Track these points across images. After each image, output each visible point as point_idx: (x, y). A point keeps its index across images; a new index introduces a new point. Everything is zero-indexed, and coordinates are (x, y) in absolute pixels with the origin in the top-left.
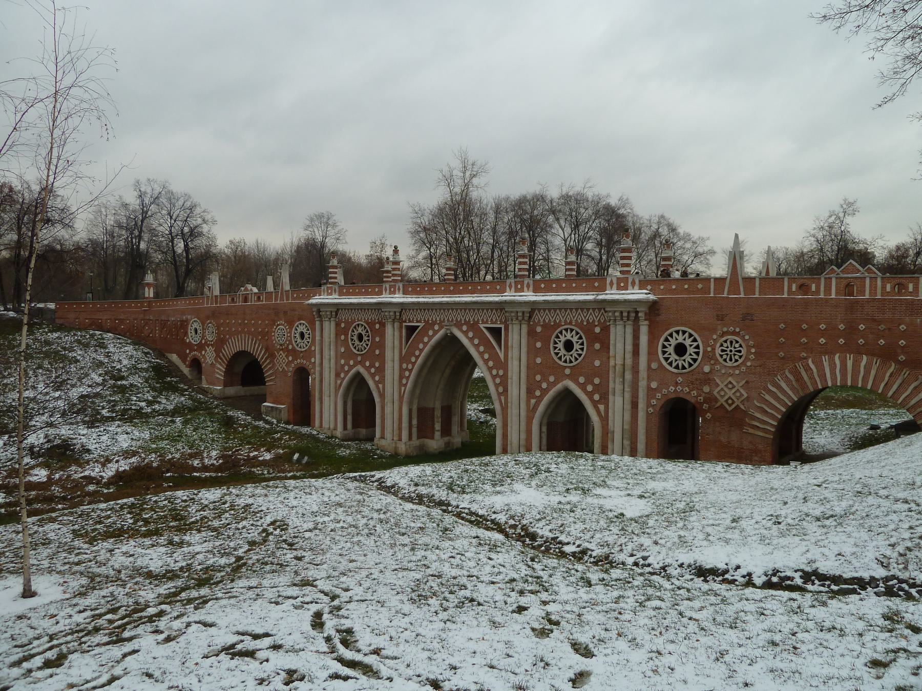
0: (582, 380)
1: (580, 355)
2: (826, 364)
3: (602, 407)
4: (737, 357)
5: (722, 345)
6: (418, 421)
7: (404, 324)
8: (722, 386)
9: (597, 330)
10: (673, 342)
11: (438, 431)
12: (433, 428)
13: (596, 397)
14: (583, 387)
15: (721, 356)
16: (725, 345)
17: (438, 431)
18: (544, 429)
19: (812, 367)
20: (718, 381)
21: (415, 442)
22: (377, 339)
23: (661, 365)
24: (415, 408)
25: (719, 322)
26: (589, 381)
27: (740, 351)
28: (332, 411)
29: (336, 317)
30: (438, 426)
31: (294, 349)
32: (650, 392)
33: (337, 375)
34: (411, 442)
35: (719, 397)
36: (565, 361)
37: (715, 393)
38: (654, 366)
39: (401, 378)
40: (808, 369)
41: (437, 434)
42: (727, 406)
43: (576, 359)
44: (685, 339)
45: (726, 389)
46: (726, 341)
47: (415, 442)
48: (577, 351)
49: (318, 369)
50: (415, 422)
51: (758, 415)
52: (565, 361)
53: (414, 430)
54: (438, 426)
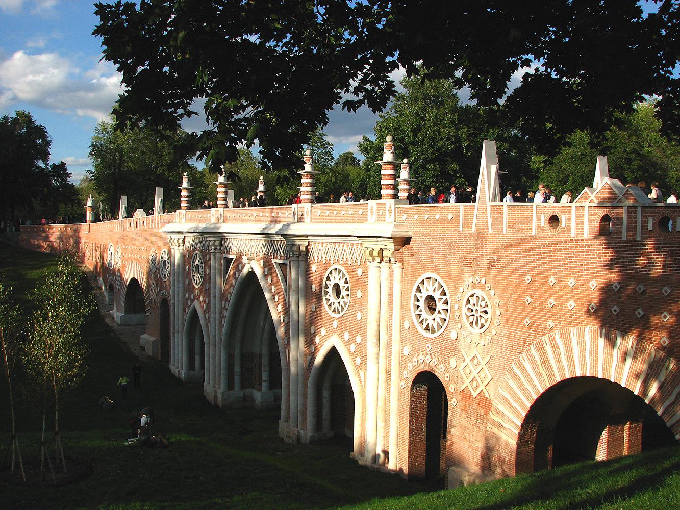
0: (347, 336)
1: (345, 303)
2: (574, 340)
3: (361, 373)
4: (483, 321)
5: (468, 302)
6: (242, 367)
7: (224, 256)
8: (468, 360)
9: (359, 272)
10: (425, 294)
11: (265, 381)
12: (260, 378)
13: (358, 361)
14: (347, 344)
15: (468, 317)
16: (472, 301)
17: (265, 381)
18: (326, 394)
19: (560, 342)
20: (464, 354)
21: (237, 392)
22: (207, 272)
23: (412, 325)
24: (237, 353)
25: (467, 269)
26: (352, 340)
27: (486, 312)
28: (180, 349)
29: (183, 246)
30: (265, 376)
31: (160, 276)
32: (403, 359)
33: (184, 310)
34: (231, 392)
35: (464, 377)
36: (334, 311)
37: (460, 369)
38: (406, 325)
39: (222, 317)
40: (555, 347)
41: (264, 386)
42: (471, 390)
43: (343, 309)
44: (434, 290)
45: (470, 364)
46: (472, 296)
47: (237, 392)
48: (343, 298)
49: (172, 302)
50: (237, 369)
51: (501, 407)
52: (334, 311)
53: (237, 379)
54: (265, 376)
